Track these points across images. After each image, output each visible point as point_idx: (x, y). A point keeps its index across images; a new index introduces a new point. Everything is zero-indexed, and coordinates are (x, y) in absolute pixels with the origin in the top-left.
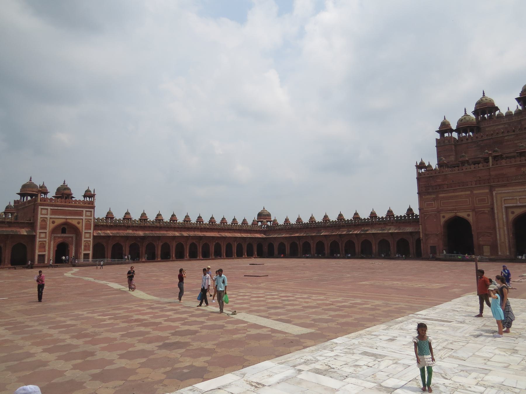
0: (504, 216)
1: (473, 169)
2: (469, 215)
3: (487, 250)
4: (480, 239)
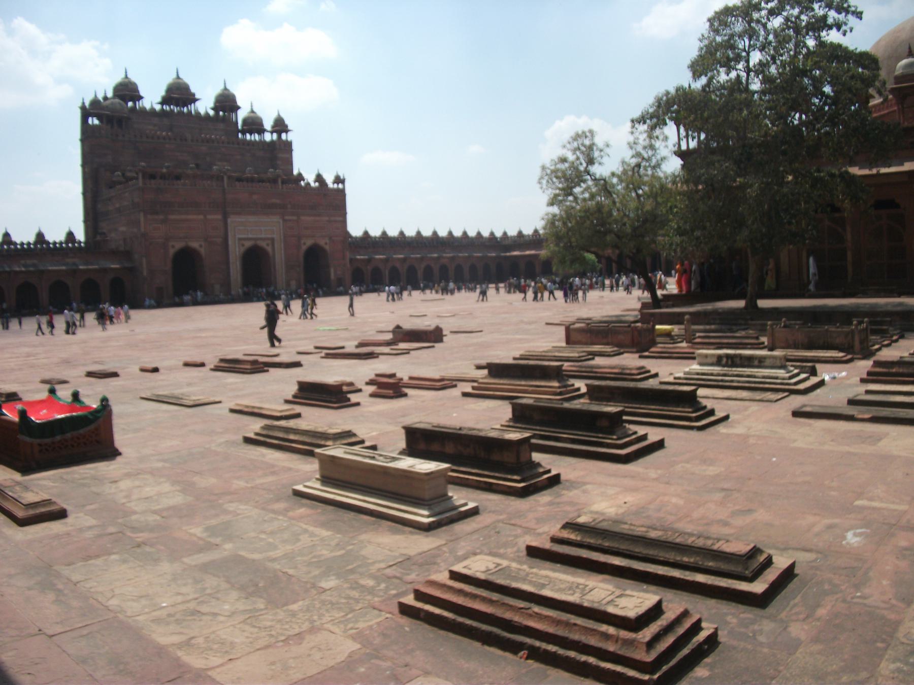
2: (201, 246)
3: (217, 287)
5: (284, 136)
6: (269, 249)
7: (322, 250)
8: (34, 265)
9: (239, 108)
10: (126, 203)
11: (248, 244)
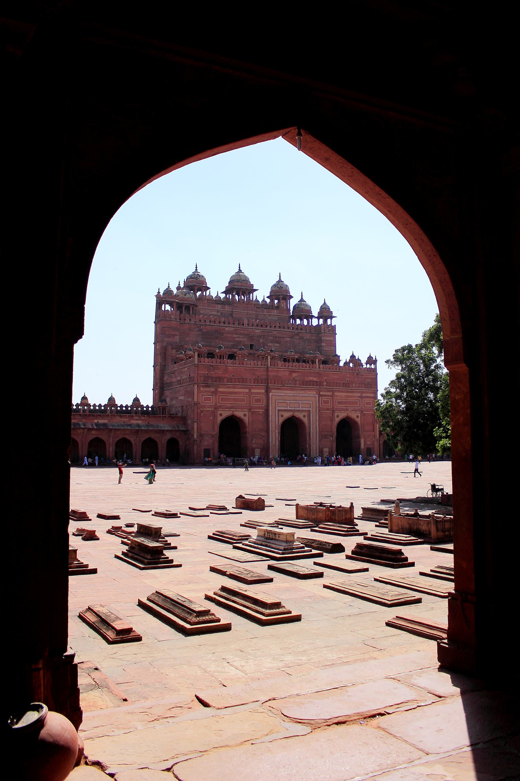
0: (277, 420)
1: (252, 365)
2: (245, 415)
3: (257, 452)
4: (253, 442)
5: (329, 321)
6: (305, 420)
7: (355, 423)
8: (105, 425)
9: (291, 297)
10: (185, 377)
11: (287, 415)
